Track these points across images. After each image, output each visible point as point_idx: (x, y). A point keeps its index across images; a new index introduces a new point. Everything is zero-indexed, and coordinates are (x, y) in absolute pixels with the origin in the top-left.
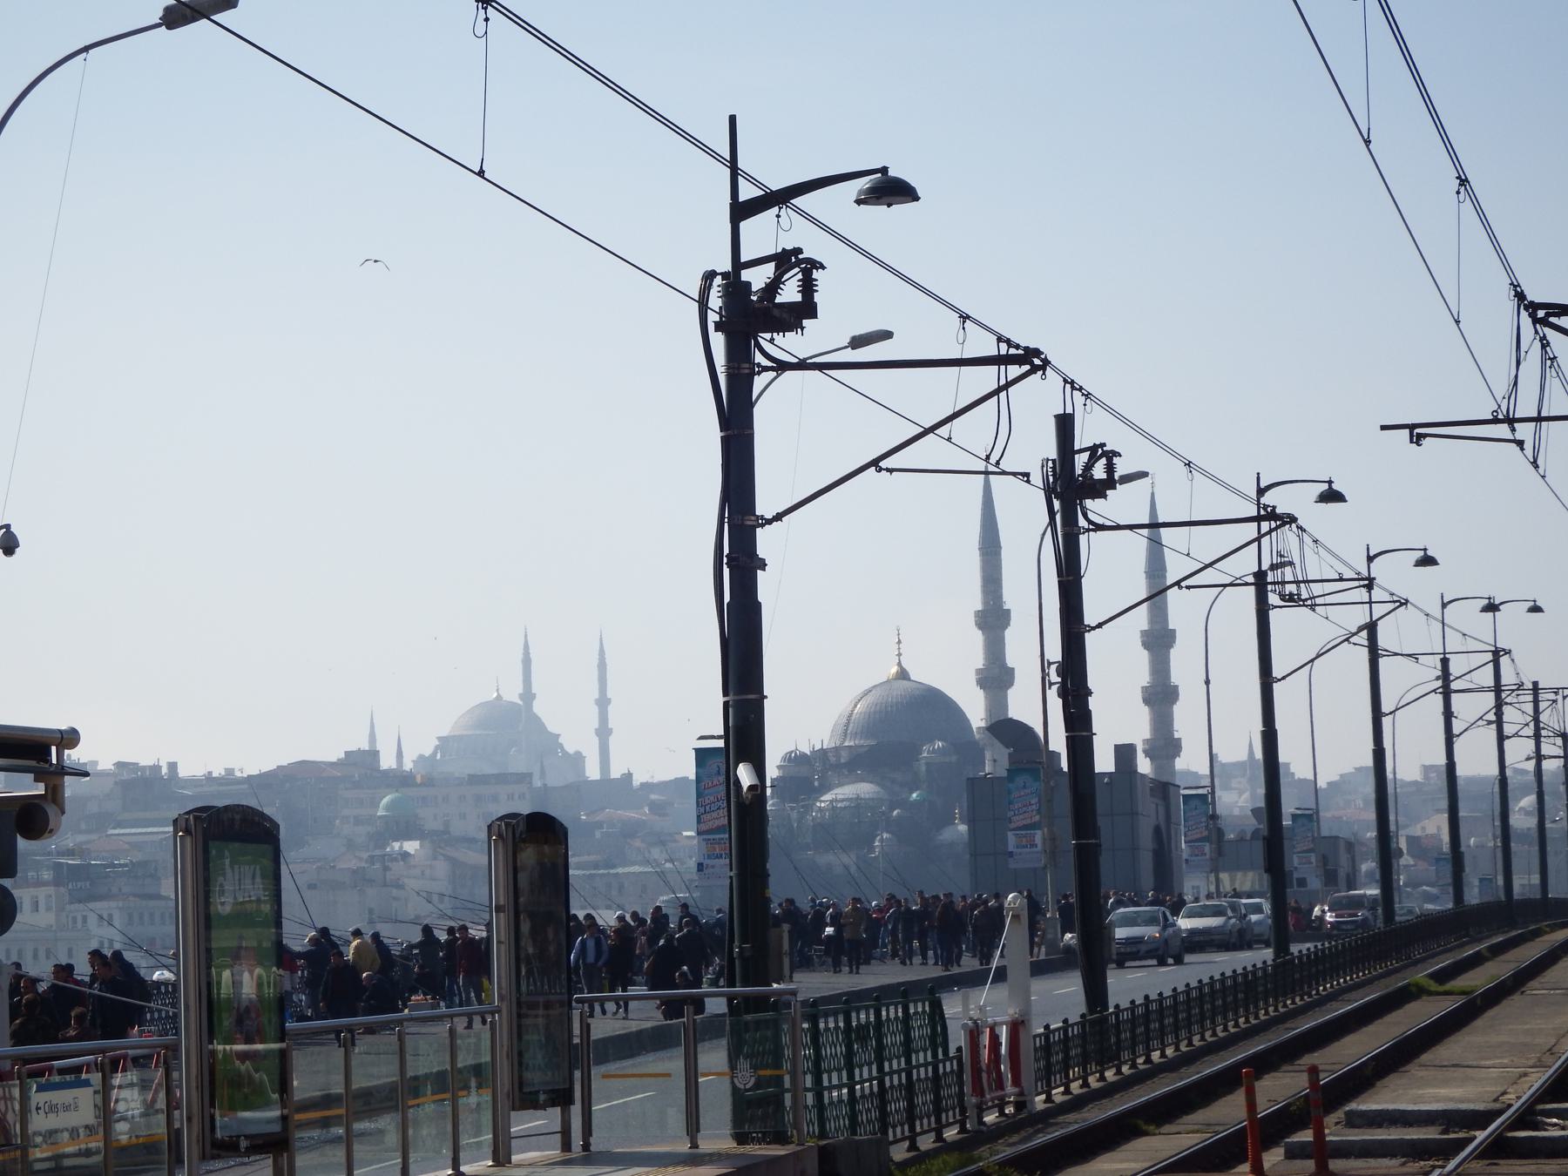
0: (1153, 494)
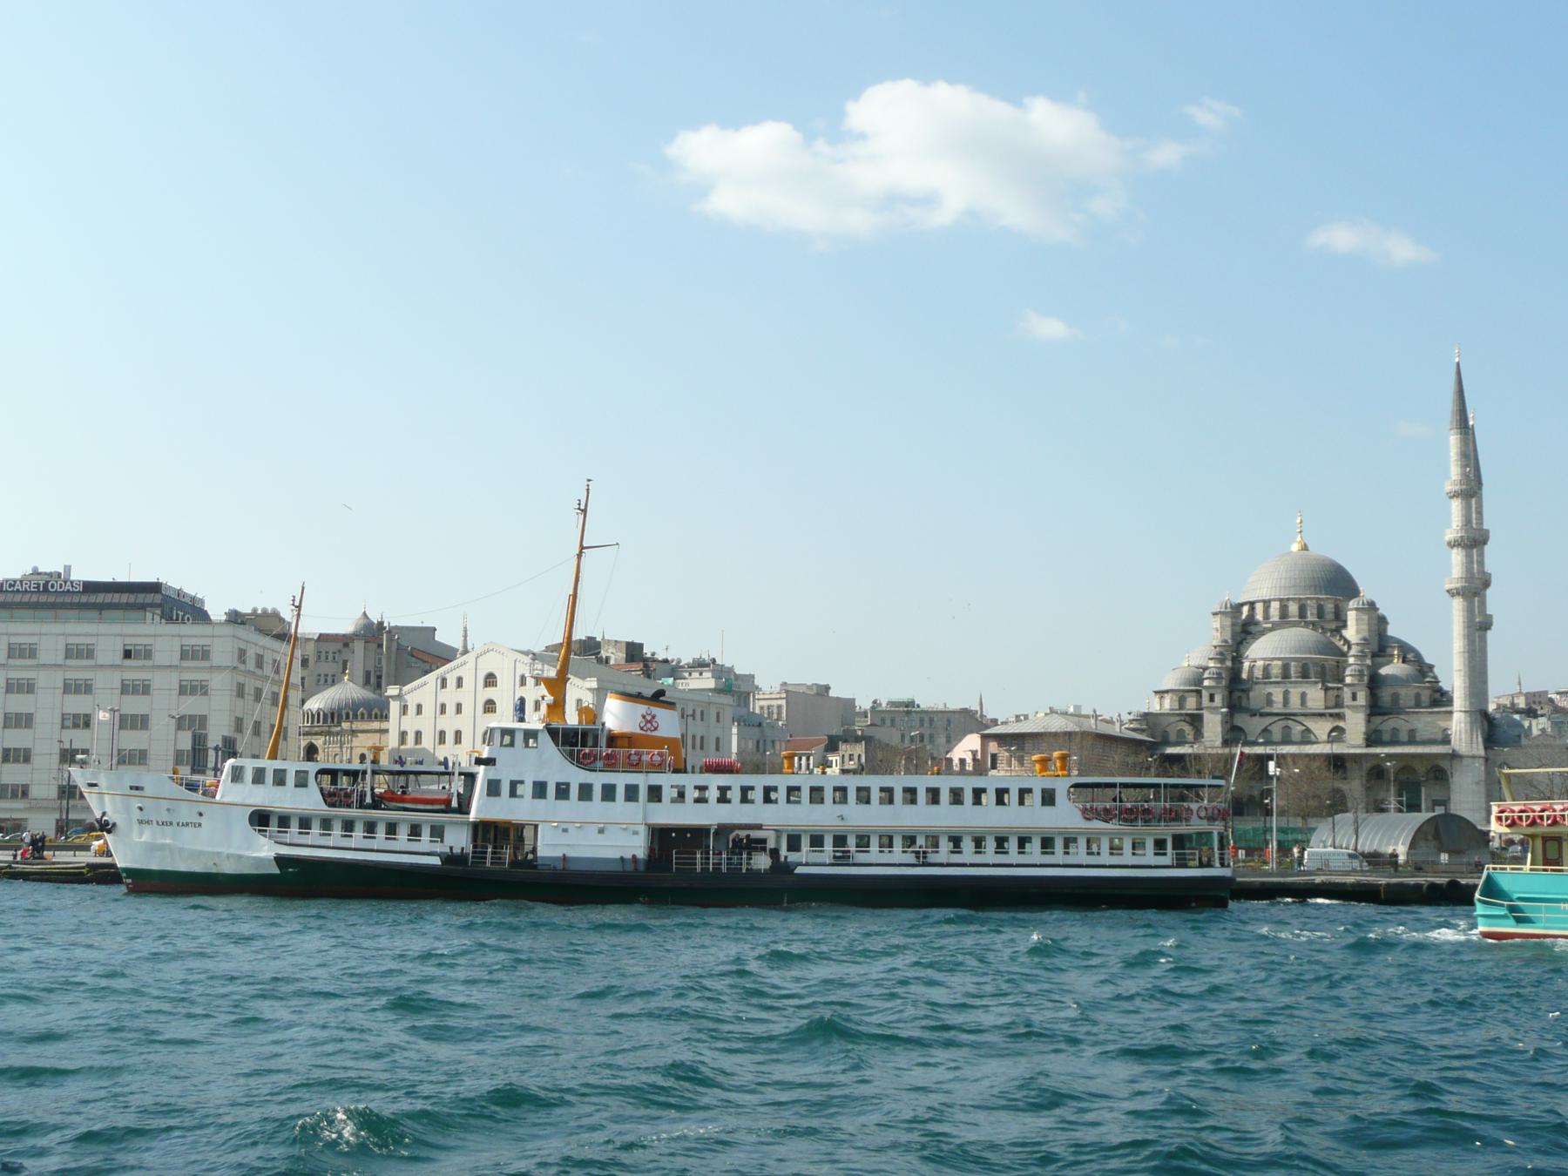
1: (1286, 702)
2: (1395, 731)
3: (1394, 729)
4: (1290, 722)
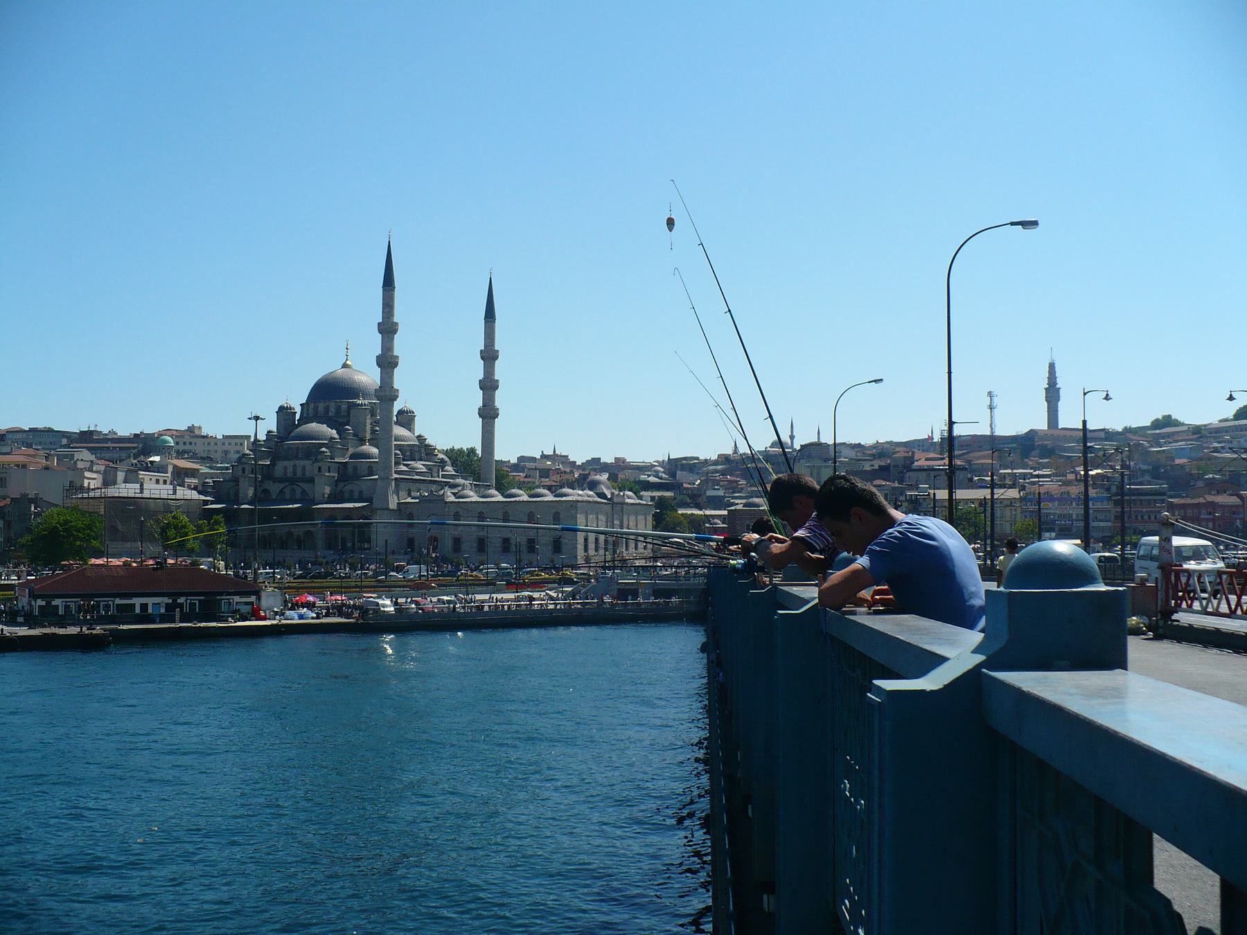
0: (491, 278)
1: (295, 473)
2: (352, 491)
3: (351, 490)
4: (295, 486)
